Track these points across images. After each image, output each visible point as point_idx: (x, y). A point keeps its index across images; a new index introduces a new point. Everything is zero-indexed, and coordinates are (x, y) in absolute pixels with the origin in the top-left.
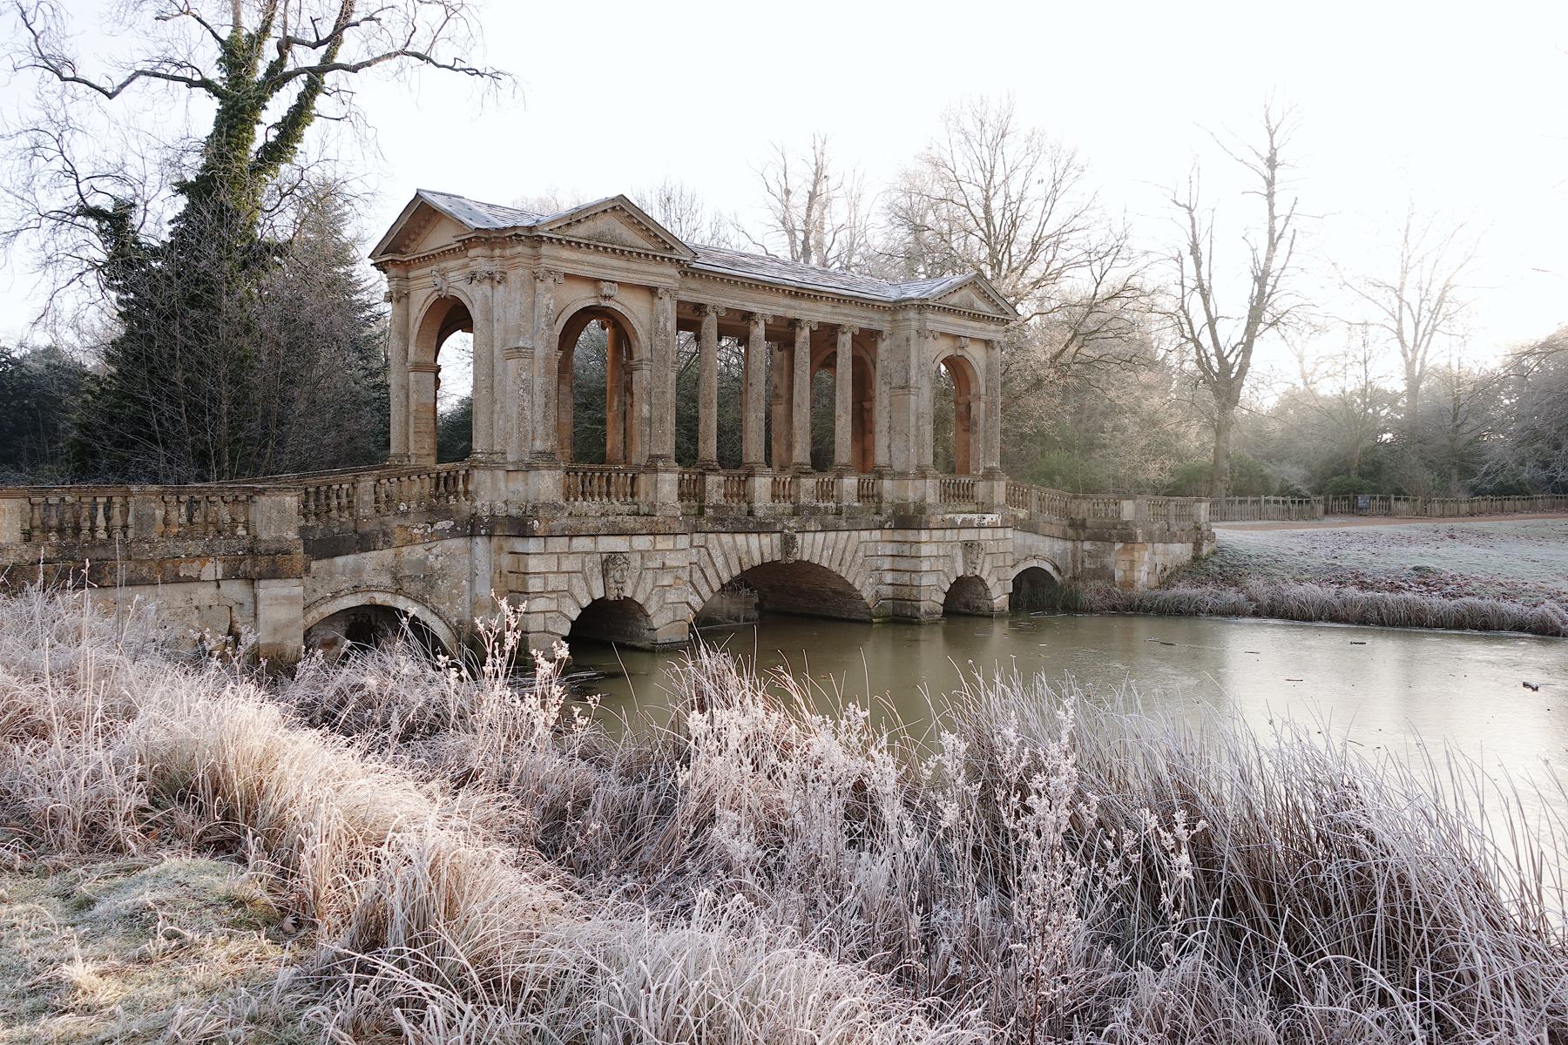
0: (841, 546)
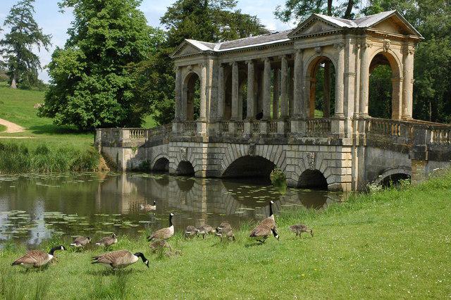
0: (274, 151)
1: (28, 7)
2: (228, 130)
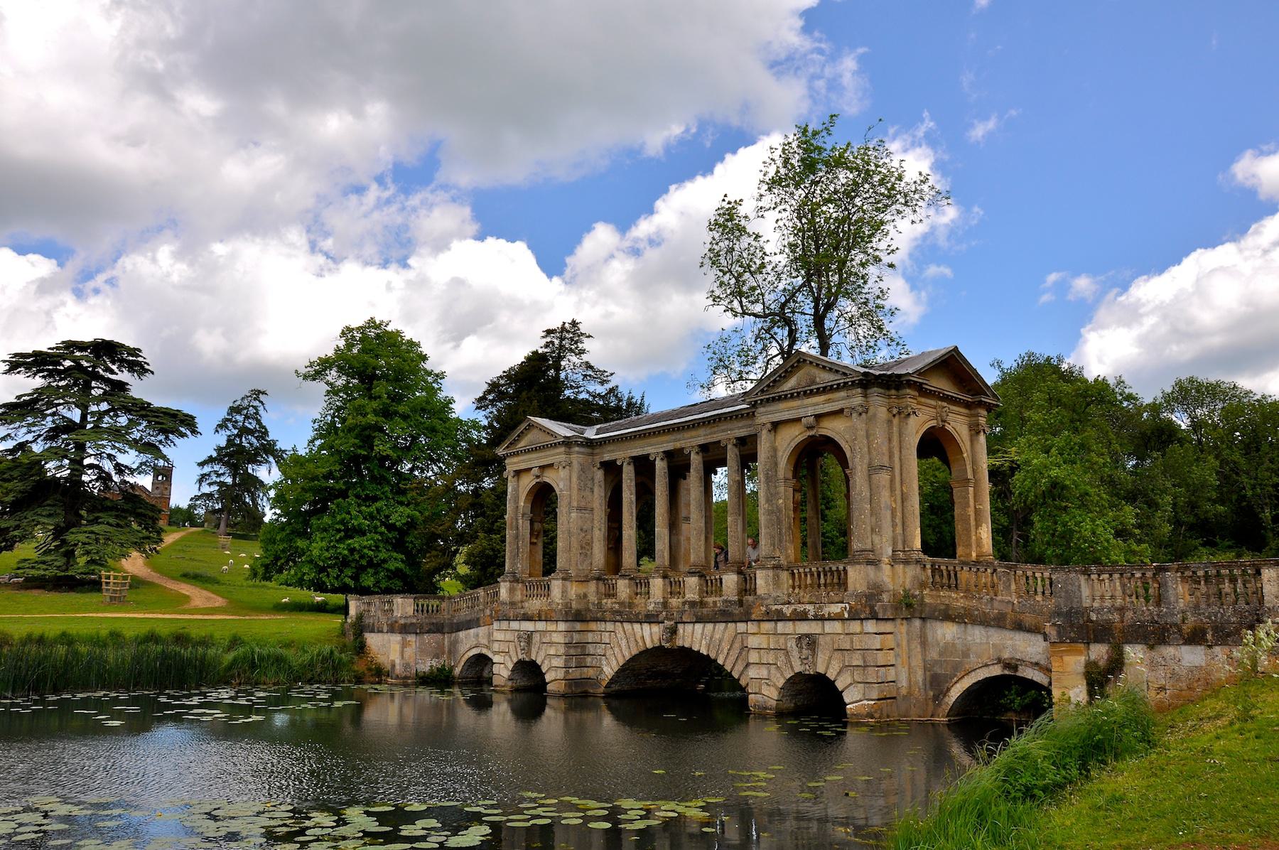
1: (256, 403)
2: (614, 595)
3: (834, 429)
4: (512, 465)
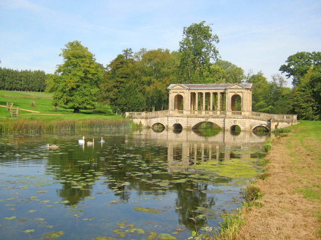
3: (240, 94)
4: (171, 92)
